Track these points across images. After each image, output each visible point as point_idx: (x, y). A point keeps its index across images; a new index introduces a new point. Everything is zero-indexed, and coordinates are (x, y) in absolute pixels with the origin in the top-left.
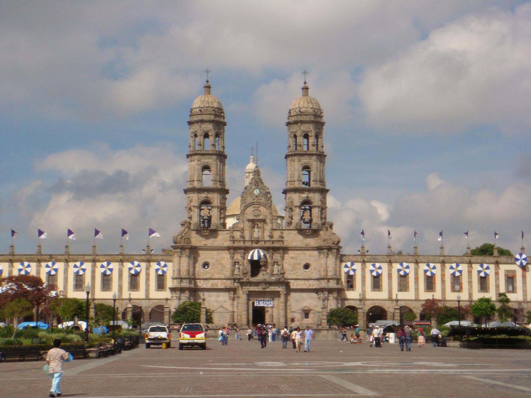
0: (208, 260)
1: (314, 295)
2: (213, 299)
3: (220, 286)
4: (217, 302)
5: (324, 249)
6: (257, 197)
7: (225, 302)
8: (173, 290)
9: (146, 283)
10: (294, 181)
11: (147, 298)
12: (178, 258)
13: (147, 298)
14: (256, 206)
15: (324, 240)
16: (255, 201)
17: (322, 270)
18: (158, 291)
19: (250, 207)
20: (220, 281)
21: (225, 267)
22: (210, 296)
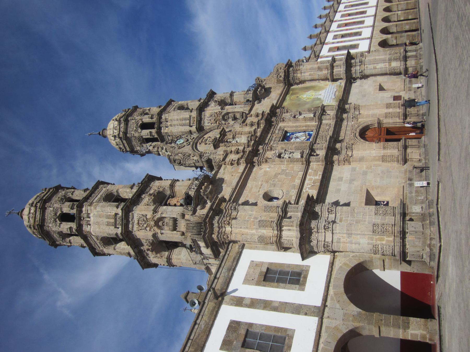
0: (262, 192)
1: (356, 87)
2: (344, 187)
3: (319, 177)
4: (351, 181)
5: (288, 72)
6: (188, 140)
7: (354, 170)
8: (307, 250)
9: (275, 309)
10: (190, 116)
11: (320, 312)
12: (234, 221)
13: (320, 312)
14: (200, 141)
15: (279, 82)
16: (191, 143)
17: (320, 73)
18: (304, 284)
19: (198, 147)
20: (308, 177)
21: (283, 170)
22: (338, 191)
